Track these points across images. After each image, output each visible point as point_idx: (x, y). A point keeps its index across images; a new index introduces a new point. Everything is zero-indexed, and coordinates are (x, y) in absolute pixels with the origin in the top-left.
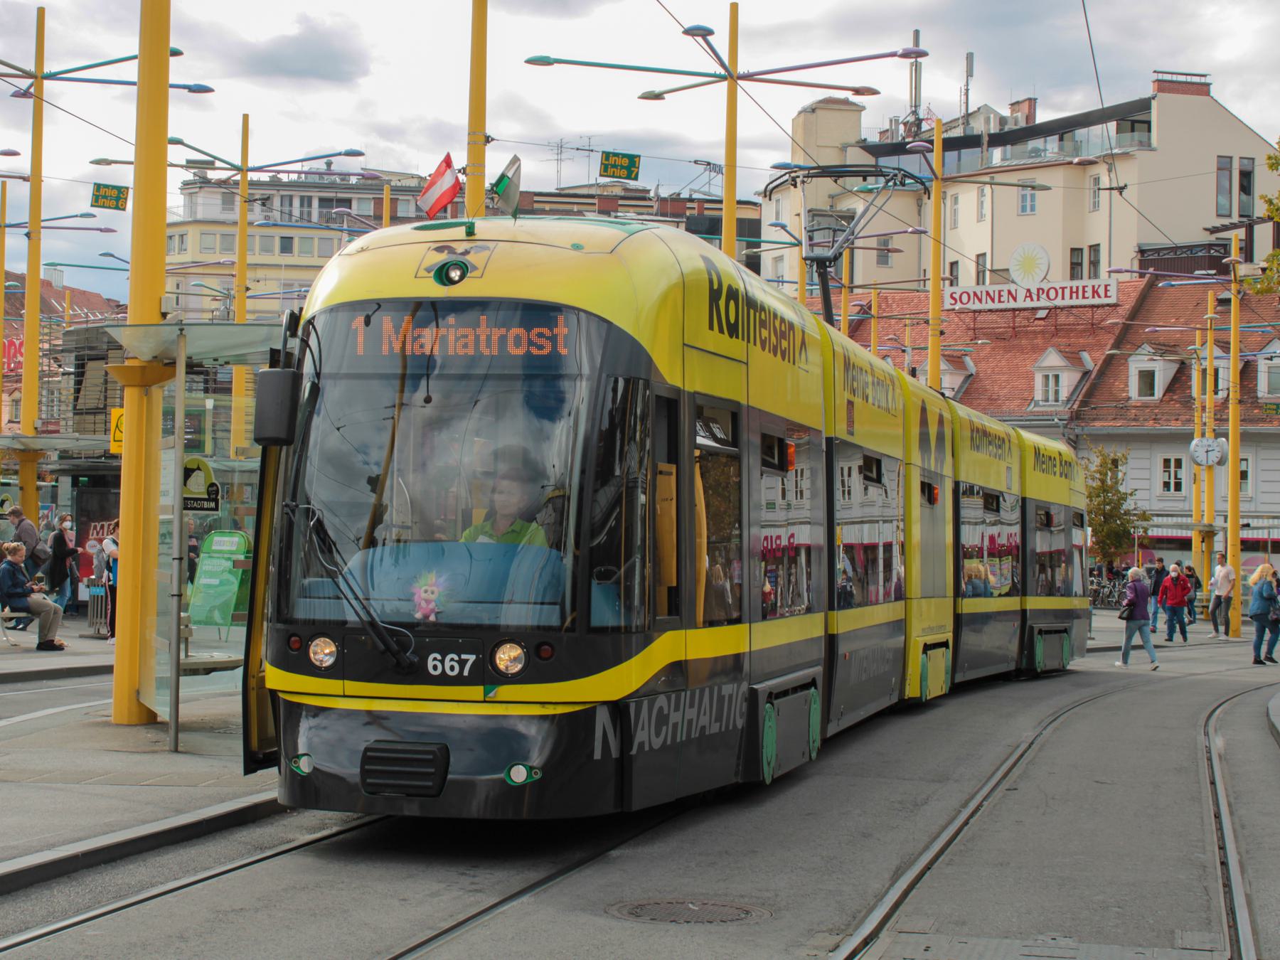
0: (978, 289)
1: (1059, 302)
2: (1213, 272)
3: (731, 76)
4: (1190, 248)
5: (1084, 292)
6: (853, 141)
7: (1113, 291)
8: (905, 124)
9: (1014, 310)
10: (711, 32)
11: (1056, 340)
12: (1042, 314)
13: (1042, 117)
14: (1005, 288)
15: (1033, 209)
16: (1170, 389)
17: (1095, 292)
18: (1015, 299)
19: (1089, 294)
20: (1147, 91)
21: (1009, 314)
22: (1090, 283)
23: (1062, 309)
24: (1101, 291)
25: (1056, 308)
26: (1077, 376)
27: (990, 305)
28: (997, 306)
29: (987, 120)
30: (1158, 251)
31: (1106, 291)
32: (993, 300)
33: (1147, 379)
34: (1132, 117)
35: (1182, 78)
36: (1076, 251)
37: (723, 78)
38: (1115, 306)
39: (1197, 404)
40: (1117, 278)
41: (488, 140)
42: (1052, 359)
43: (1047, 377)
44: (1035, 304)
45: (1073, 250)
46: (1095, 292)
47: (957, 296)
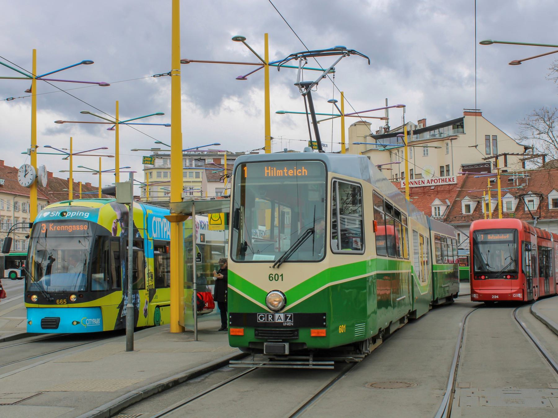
0: (412, 181)
1: (438, 184)
3: (342, 115)
4: (478, 165)
6: (368, 134)
7: (455, 180)
8: (384, 128)
10: (336, 101)
12: (433, 188)
13: (428, 124)
14: (421, 180)
15: (427, 154)
16: (475, 210)
17: (449, 180)
19: (448, 181)
21: (422, 188)
22: (448, 177)
23: (439, 186)
24: (452, 180)
26: (445, 207)
27: (416, 186)
28: (418, 186)
29: (411, 126)
30: (468, 166)
33: (468, 207)
34: (458, 124)
36: (442, 167)
37: (339, 116)
38: (456, 184)
39: (485, 215)
40: (456, 174)
41: (272, 138)
42: (437, 202)
43: (436, 208)
45: (441, 167)
46: (449, 180)
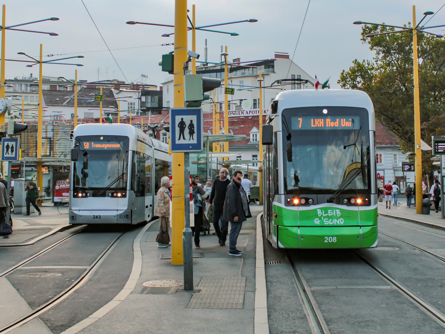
12: (250, 118)
20: (273, 58)
23: (256, 116)
25: (254, 116)
34: (269, 64)
35: (282, 54)
43: (253, 135)
44: (249, 115)
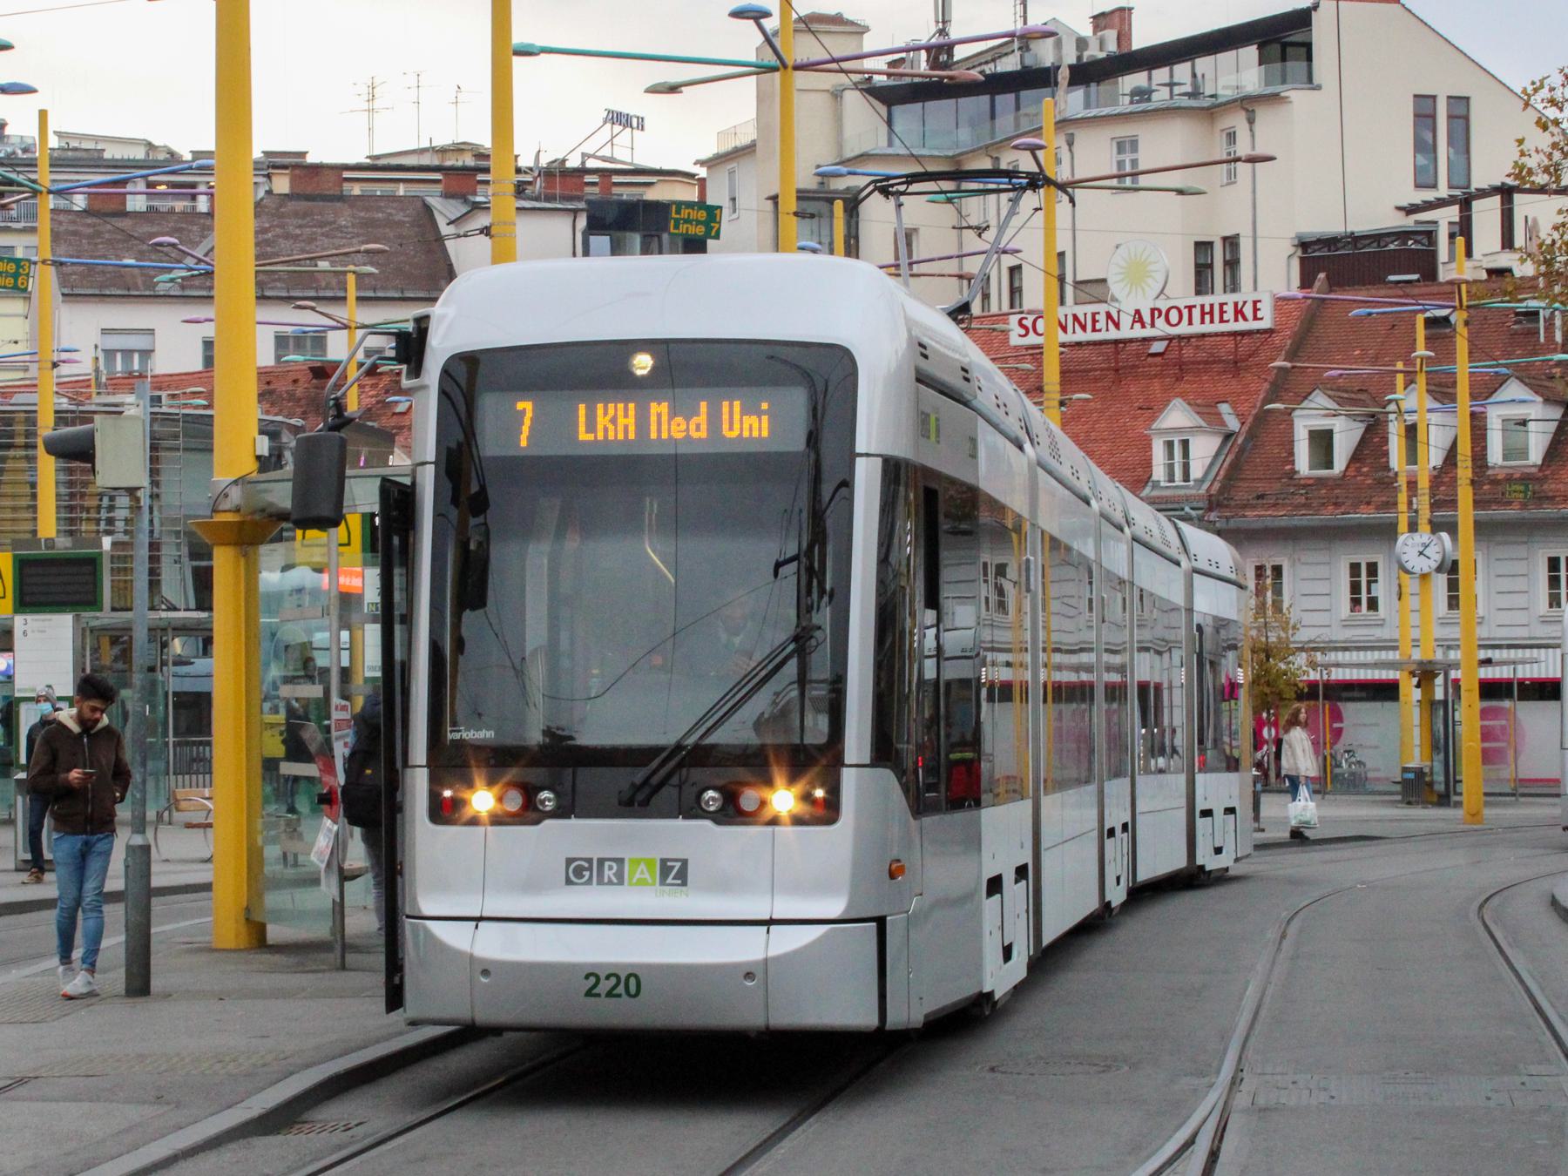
1: (1183, 329)
2: (1415, 277)
5: (1222, 312)
7: (1266, 311)
9: (1116, 342)
11: (1183, 386)
14: (1102, 308)
17: (1238, 312)
18: (1117, 326)
19: (1229, 315)
22: (1230, 298)
24: (1248, 311)
25: (1180, 338)
31: (1256, 310)
32: (1084, 328)
36: (1203, 247)
38: (1269, 331)
42: (1177, 416)
43: (1170, 445)
44: (1148, 332)
45: (1198, 245)
46: (1238, 312)
47: (1028, 323)
